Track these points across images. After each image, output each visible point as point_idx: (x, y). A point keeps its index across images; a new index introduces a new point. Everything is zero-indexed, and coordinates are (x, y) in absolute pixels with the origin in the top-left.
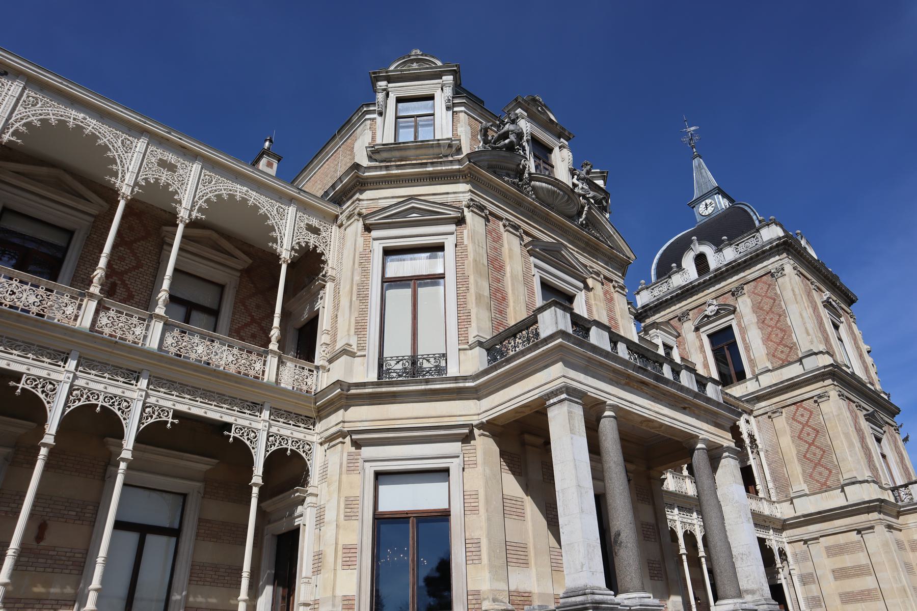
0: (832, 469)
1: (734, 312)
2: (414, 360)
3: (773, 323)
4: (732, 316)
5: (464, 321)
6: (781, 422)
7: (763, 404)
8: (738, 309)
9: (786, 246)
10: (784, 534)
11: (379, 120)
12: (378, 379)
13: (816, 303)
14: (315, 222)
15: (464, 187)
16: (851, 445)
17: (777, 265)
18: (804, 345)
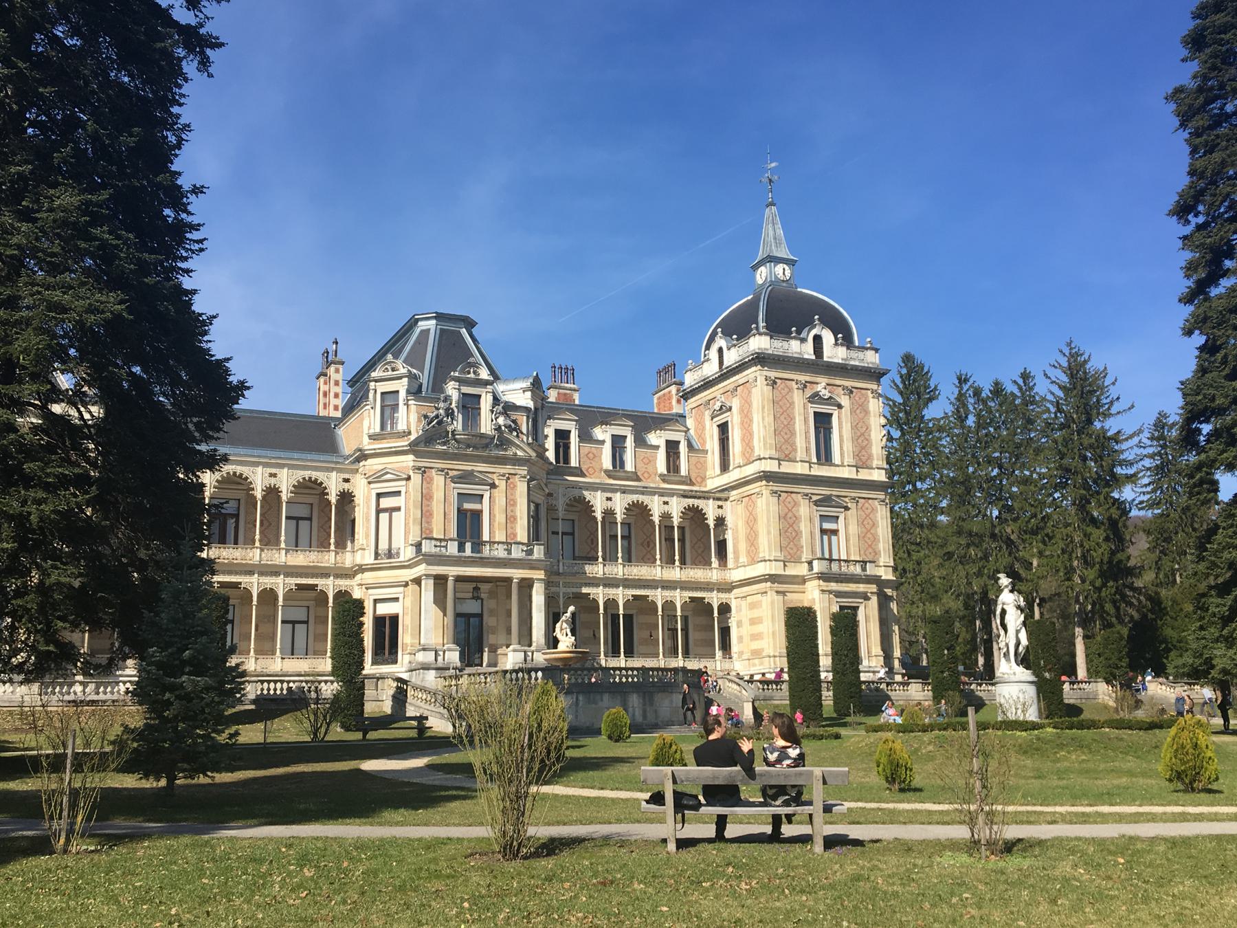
0: (757, 552)
1: (730, 409)
2: (390, 550)
3: (746, 426)
4: (728, 413)
5: (407, 533)
6: (740, 508)
7: (734, 492)
8: (734, 409)
9: (760, 359)
10: (735, 591)
11: (372, 411)
12: (376, 558)
13: (792, 404)
14: (347, 476)
15: (411, 457)
16: (769, 533)
17: (752, 376)
18: (759, 451)
